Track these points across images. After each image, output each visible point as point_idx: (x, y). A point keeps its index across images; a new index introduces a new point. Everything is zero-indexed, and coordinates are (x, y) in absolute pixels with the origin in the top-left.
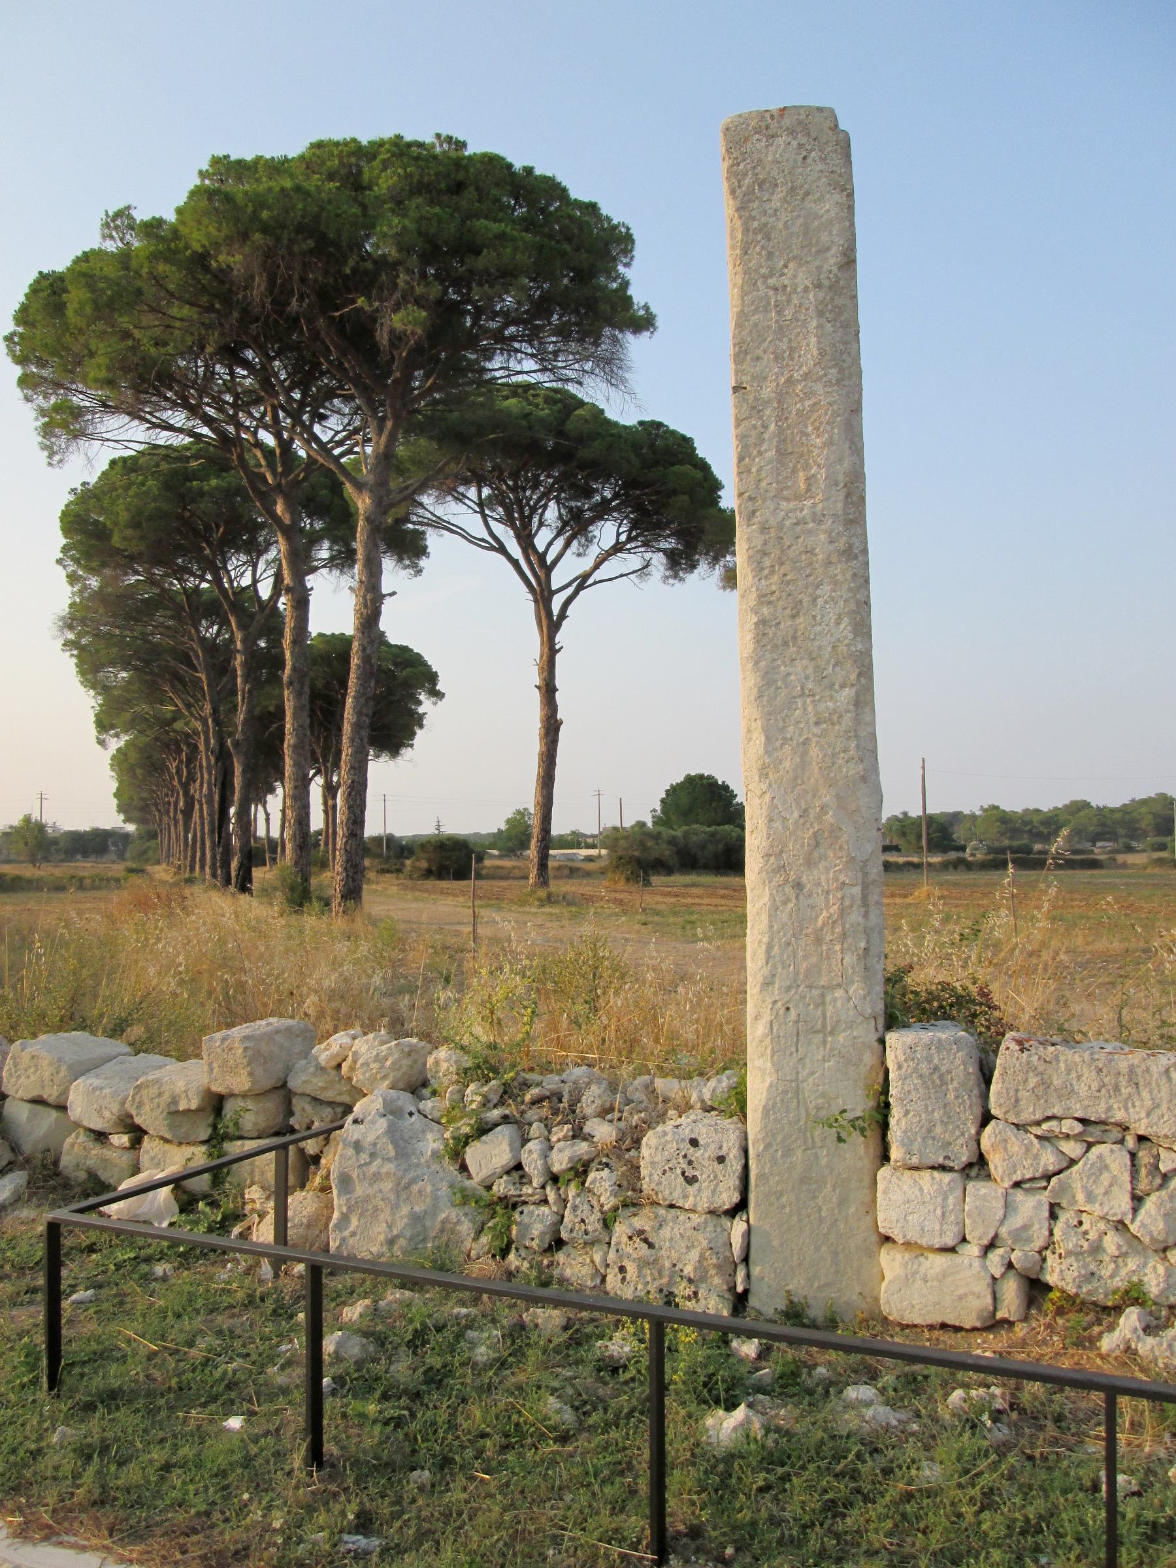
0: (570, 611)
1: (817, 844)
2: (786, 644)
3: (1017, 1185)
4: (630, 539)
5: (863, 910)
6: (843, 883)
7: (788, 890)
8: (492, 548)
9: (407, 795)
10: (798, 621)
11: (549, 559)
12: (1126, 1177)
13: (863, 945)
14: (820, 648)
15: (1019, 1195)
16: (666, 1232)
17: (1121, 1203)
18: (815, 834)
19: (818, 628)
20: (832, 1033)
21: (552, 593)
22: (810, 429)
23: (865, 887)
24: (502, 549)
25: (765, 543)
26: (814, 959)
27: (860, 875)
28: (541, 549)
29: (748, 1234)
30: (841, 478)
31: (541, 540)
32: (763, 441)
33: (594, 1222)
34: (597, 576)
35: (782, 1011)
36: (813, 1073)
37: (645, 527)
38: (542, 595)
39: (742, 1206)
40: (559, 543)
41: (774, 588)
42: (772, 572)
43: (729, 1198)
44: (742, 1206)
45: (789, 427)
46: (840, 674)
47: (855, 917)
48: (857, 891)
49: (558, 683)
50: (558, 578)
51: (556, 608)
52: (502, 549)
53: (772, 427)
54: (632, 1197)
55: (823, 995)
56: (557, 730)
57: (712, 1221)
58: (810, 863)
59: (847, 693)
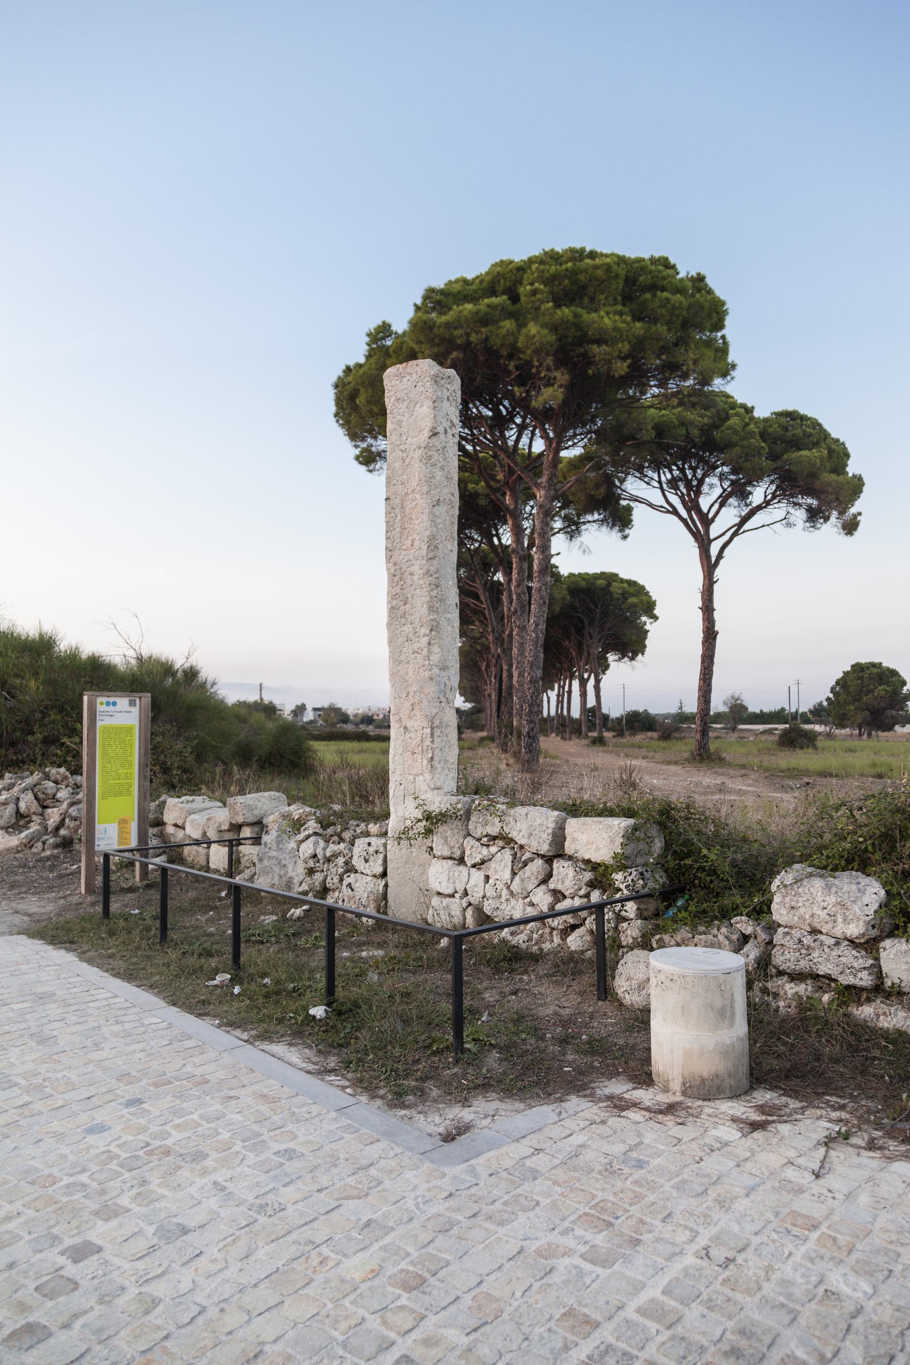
0: (726, 553)
3: (474, 866)
4: (774, 497)
8: (668, 512)
9: (624, 685)
11: (711, 516)
12: (510, 864)
15: (473, 870)
16: (357, 885)
17: (507, 875)
21: (710, 541)
23: (432, 729)
24: (675, 512)
28: (705, 510)
29: (386, 886)
30: (426, 539)
33: (336, 880)
34: (747, 526)
37: (790, 485)
38: (704, 542)
39: (384, 874)
40: (716, 506)
43: (379, 870)
44: (384, 874)
47: (427, 742)
48: (428, 731)
49: (716, 604)
50: (714, 530)
51: (714, 549)
52: (675, 512)
54: (350, 869)
56: (715, 638)
57: (375, 880)
58: (410, 717)
59: (426, 639)
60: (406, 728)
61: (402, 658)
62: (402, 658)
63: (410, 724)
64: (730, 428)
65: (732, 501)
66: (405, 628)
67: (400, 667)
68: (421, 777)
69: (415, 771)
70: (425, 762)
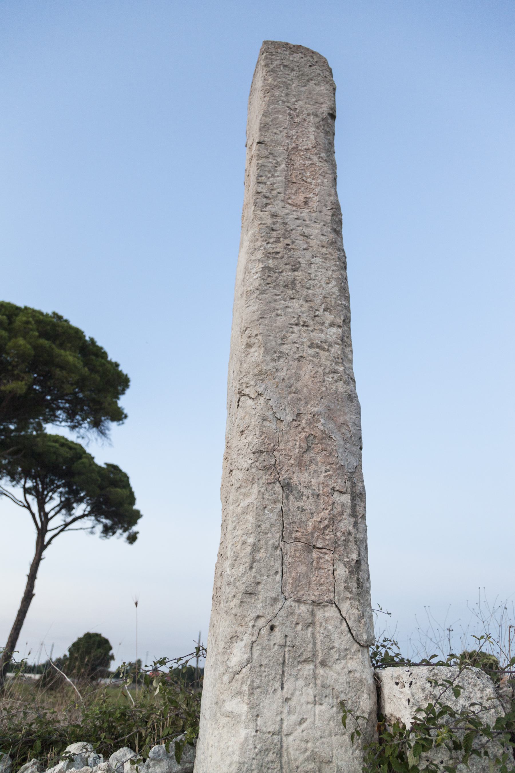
1: (308, 449)
2: (286, 286)
5: (352, 520)
6: (333, 489)
7: (277, 487)
8: (24, 506)
10: (296, 273)
13: (354, 556)
14: (314, 295)
18: (307, 438)
19: (312, 282)
20: (323, 664)
22: (308, 174)
24: (29, 507)
25: (274, 223)
26: (302, 569)
27: (348, 484)
31: (48, 507)
32: (276, 171)
35: (265, 631)
36: (302, 721)
38: (42, 532)
41: (278, 250)
42: (278, 241)
45: (294, 169)
46: (329, 317)
52: (29, 507)
53: (283, 166)
55: (313, 614)
58: (301, 464)
60: (287, 486)
61: (285, 349)
62: (285, 349)
63: (299, 478)
64: (82, 463)
65: (63, 511)
66: (295, 304)
67: (281, 363)
68: (331, 612)
69: (313, 595)
70: (342, 571)
